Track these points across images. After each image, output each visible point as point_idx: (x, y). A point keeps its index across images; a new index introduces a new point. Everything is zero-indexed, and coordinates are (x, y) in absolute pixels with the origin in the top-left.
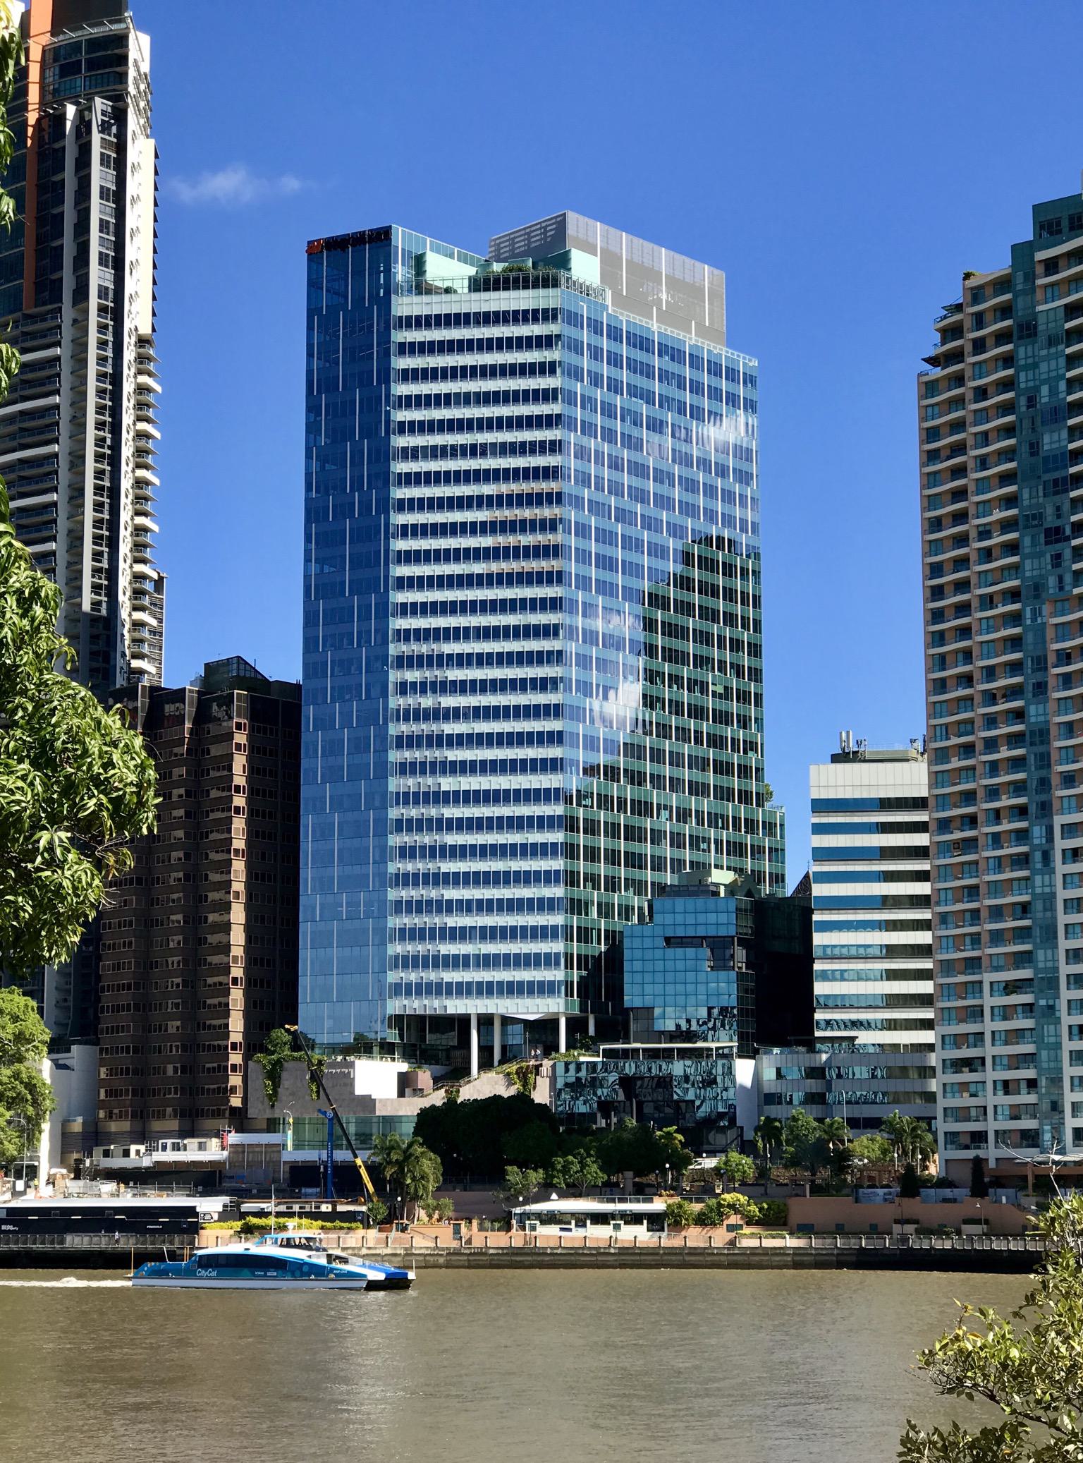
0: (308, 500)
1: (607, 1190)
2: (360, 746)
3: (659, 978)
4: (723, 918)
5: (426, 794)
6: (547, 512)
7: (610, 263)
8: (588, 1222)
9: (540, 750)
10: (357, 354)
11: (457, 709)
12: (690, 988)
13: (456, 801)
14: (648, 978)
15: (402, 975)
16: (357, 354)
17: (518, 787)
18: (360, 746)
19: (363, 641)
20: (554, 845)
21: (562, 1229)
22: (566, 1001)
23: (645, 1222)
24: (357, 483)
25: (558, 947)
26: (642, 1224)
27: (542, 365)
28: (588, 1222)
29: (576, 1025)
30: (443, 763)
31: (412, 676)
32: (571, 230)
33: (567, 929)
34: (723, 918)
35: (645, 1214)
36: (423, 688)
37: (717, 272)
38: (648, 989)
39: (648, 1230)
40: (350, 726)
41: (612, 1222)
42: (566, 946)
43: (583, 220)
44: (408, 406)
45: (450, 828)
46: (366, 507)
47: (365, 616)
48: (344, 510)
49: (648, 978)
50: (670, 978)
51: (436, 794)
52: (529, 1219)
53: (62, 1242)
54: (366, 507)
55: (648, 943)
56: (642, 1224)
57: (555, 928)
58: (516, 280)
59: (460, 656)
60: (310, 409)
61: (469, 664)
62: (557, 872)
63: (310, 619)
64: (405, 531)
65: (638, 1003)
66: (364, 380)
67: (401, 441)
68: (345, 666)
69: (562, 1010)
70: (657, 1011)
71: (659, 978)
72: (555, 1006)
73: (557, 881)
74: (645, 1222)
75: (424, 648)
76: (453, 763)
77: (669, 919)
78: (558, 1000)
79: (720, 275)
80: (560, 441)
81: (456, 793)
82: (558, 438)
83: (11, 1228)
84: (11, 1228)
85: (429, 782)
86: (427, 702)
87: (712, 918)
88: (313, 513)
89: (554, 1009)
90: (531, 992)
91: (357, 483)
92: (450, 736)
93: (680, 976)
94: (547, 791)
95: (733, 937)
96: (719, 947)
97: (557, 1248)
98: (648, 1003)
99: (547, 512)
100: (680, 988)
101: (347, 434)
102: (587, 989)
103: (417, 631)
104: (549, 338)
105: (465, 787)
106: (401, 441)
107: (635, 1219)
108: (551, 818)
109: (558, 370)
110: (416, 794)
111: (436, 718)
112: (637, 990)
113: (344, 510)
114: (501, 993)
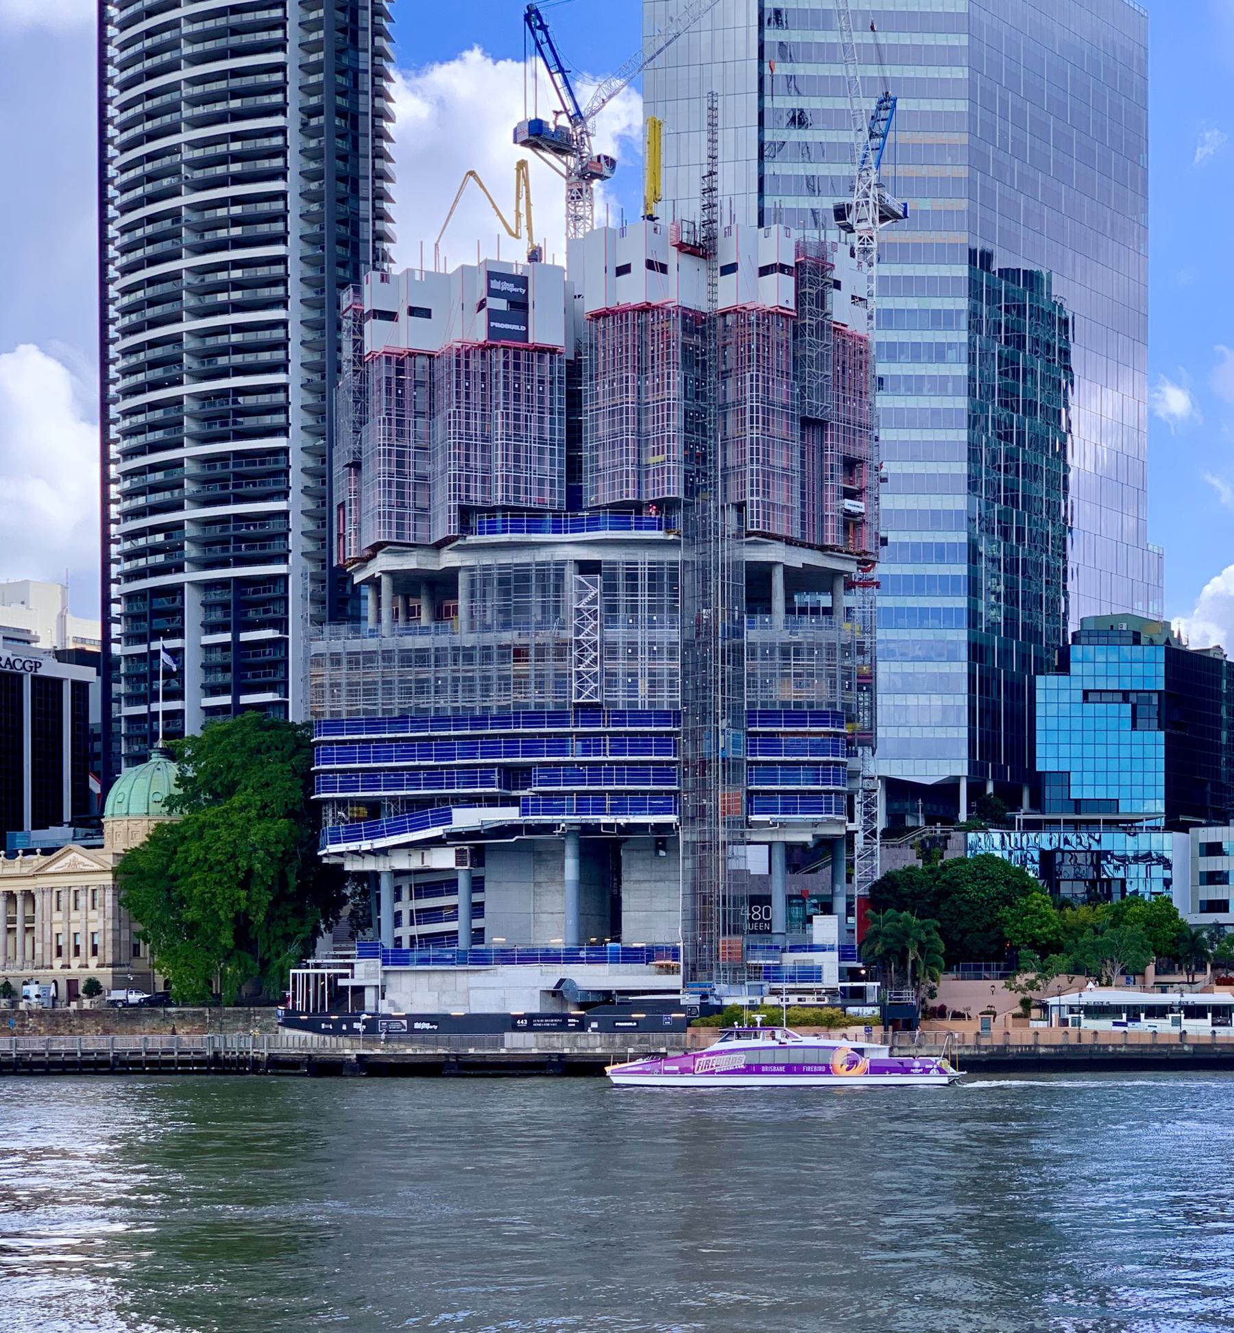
3: (1077, 738)
8: (1142, 1015)
12: (1113, 751)
14: (1064, 737)
23: (1210, 1015)
26: (1206, 1017)
28: (1142, 1015)
29: (975, 790)
38: (1064, 750)
39: (1213, 1025)
49: (1064, 737)
50: (1089, 737)
55: (1065, 697)
56: (1206, 1017)
70: (1074, 778)
71: (1077, 738)
74: (1210, 1015)
77: (1089, 668)
83: (427, 1026)
84: (427, 1026)
93: (1101, 737)
100: (1101, 750)
107: (1195, 1012)
112: (1051, 751)
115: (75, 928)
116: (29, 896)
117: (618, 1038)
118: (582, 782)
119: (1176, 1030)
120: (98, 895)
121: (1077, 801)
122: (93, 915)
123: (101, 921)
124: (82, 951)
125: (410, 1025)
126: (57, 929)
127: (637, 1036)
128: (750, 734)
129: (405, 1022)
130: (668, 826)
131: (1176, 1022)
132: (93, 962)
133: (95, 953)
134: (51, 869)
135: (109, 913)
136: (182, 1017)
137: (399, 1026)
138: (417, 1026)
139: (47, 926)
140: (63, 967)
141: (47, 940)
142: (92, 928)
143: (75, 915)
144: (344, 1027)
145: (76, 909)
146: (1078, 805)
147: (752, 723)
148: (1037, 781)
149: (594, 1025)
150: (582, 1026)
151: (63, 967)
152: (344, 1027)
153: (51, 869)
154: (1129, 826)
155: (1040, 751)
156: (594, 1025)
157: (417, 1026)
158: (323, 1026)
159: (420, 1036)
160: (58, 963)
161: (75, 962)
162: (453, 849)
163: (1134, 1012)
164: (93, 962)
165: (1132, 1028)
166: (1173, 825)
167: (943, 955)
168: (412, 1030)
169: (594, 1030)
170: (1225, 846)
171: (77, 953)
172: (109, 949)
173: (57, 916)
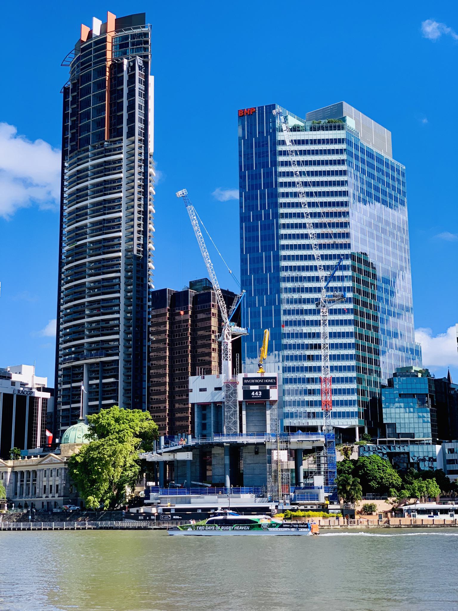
0: (241, 213)
1: (443, 499)
2: (267, 313)
4: (423, 386)
5: (297, 334)
6: (342, 220)
7: (357, 124)
8: (439, 513)
9: (344, 316)
10: (262, 154)
11: (308, 299)
13: (310, 337)
15: (298, 409)
16: (262, 154)
17: (344, 331)
18: (267, 313)
19: (268, 271)
20: (351, 355)
21: (429, 516)
22: (359, 420)
24: (263, 206)
25: (354, 397)
27: (339, 161)
28: (439, 513)
29: (361, 430)
30: (304, 321)
31: (289, 285)
32: (344, 110)
33: (358, 390)
34: (423, 386)
35: (432, 509)
36: (294, 290)
37: (389, 131)
40: (263, 305)
41: (449, 513)
42: (358, 398)
43: (348, 105)
44: (284, 176)
45: (307, 348)
46: (267, 216)
47: (268, 259)
48: (258, 217)
51: (301, 334)
52: (412, 512)
54: (267, 216)
57: (353, 389)
58: (331, 127)
59: (309, 277)
60: (241, 177)
61: (313, 281)
62: (353, 366)
63: (243, 261)
64: (284, 226)
65: (389, 421)
66: (265, 165)
67: (281, 190)
68: (260, 281)
69: (357, 424)
72: (354, 422)
73: (353, 370)
75: (294, 274)
76: (308, 321)
78: (355, 420)
79: (390, 133)
80: (347, 191)
81: (309, 334)
82: (347, 190)
83: (178, 517)
84: (178, 517)
85: (297, 329)
86: (296, 296)
87: (418, 386)
88: (244, 218)
89: (354, 424)
90: (344, 416)
91: (263, 206)
92: (306, 310)
94: (348, 333)
95: (427, 394)
96: (421, 398)
97: (432, 525)
98: (393, 421)
99: (342, 220)
101: (258, 186)
102: (366, 415)
103: (291, 267)
104: (341, 150)
105: (313, 331)
106: (281, 190)
108: (349, 344)
109: (345, 163)
110: (293, 334)
111: (300, 302)
113: (258, 217)
114: (339, 416)
115: (51, 483)
116: (35, 472)
119: (452, 519)
120: (59, 471)
121: (399, 434)
122: (57, 478)
123: (60, 480)
124: (53, 491)
125: (172, 517)
126: (45, 484)
129: (170, 516)
131: (452, 516)
132: (57, 495)
133: (57, 492)
134: (43, 462)
135: (63, 478)
137: (168, 517)
138: (174, 517)
139: (41, 483)
140: (46, 497)
141: (41, 487)
142: (57, 483)
143: (51, 479)
144: (148, 518)
145: (51, 476)
146: (398, 435)
148: (383, 426)
151: (46, 497)
152: (148, 518)
153: (43, 462)
154: (420, 443)
155: (384, 416)
157: (174, 517)
158: (140, 518)
160: (44, 496)
161: (50, 496)
163: (435, 512)
164: (57, 495)
165: (435, 518)
166: (435, 442)
167: (362, 491)
168: (172, 519)
170: (455, 450)
171: (51, 493)
172: (62, 491)
173: (45, 479)
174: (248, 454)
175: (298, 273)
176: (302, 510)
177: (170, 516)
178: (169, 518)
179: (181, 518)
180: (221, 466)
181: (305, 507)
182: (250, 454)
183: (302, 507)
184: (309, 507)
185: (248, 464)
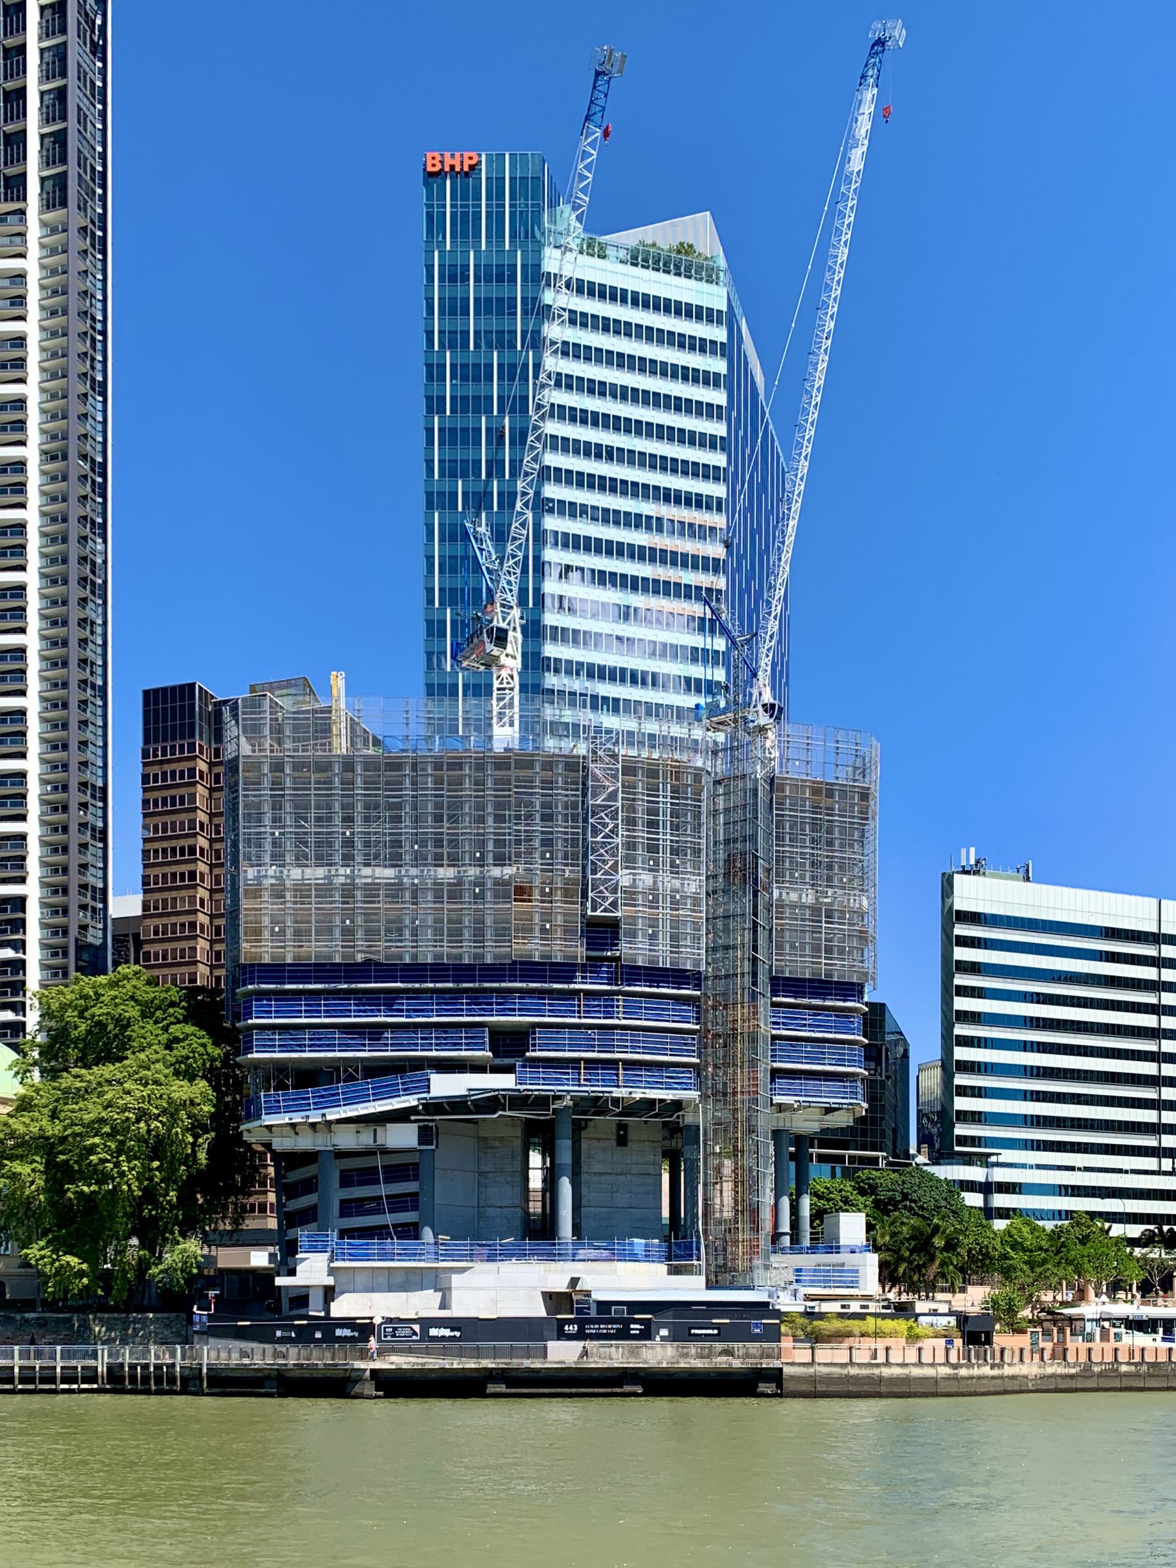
53: (544, 1353)
83: (447, 1332)
84: (447, 1332)
117: (693, 1348)
118: (591, 1048)
127: (719, 1346)
128: (773, 1005)
129: (417, 1328)
130: (678, 1105)
136: (42, 1324)
137: (407, 1332)
138: (433, 1332)
144: (318, 1335)
147: (774, 993)
149: (664, 1332)
150: (646, 1334)
156: (664, 1332)
157: (433, 1332)
158: (279, 1334)
159: (440, 1345)
162: (416, 1125)
169: (663, 1338)
174: (595, 1143)
175: (588, 684)
176: (841, 1316)
177: (417, 1328)
178: (415, 1333)
179: (458, 1334)
180: (509, 1179)
181: (843, 1307)
182: (601, 1144)
183: (835, 1307)
184: (855, 1307)
185: (595, 1174)
